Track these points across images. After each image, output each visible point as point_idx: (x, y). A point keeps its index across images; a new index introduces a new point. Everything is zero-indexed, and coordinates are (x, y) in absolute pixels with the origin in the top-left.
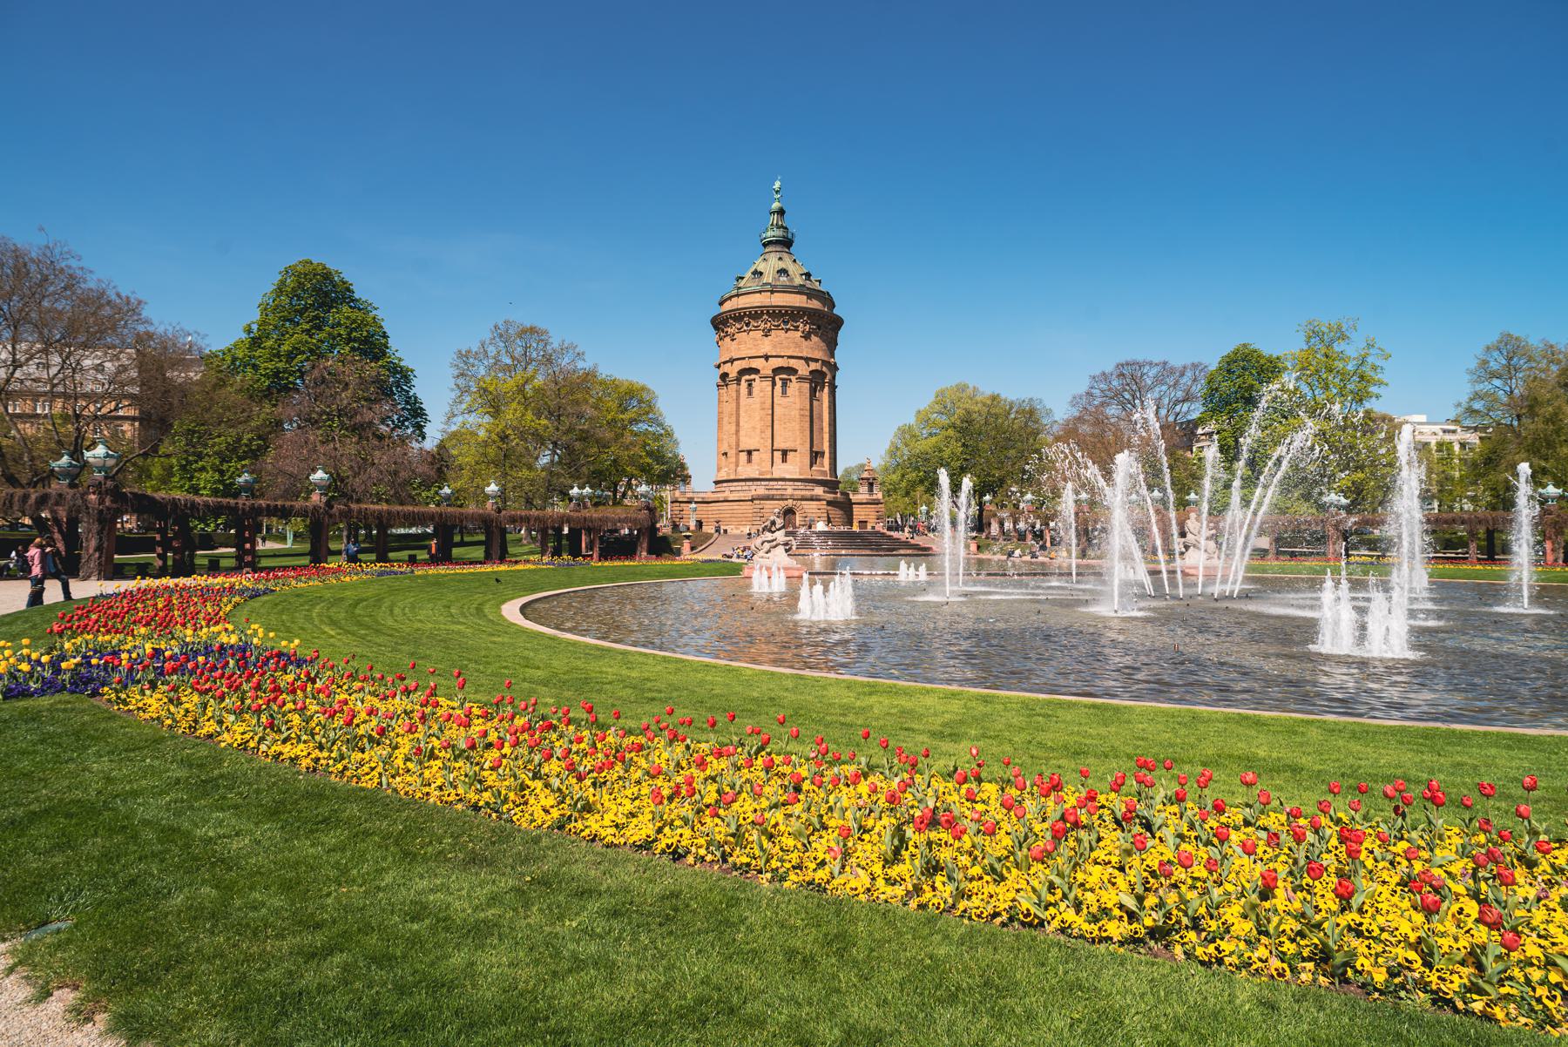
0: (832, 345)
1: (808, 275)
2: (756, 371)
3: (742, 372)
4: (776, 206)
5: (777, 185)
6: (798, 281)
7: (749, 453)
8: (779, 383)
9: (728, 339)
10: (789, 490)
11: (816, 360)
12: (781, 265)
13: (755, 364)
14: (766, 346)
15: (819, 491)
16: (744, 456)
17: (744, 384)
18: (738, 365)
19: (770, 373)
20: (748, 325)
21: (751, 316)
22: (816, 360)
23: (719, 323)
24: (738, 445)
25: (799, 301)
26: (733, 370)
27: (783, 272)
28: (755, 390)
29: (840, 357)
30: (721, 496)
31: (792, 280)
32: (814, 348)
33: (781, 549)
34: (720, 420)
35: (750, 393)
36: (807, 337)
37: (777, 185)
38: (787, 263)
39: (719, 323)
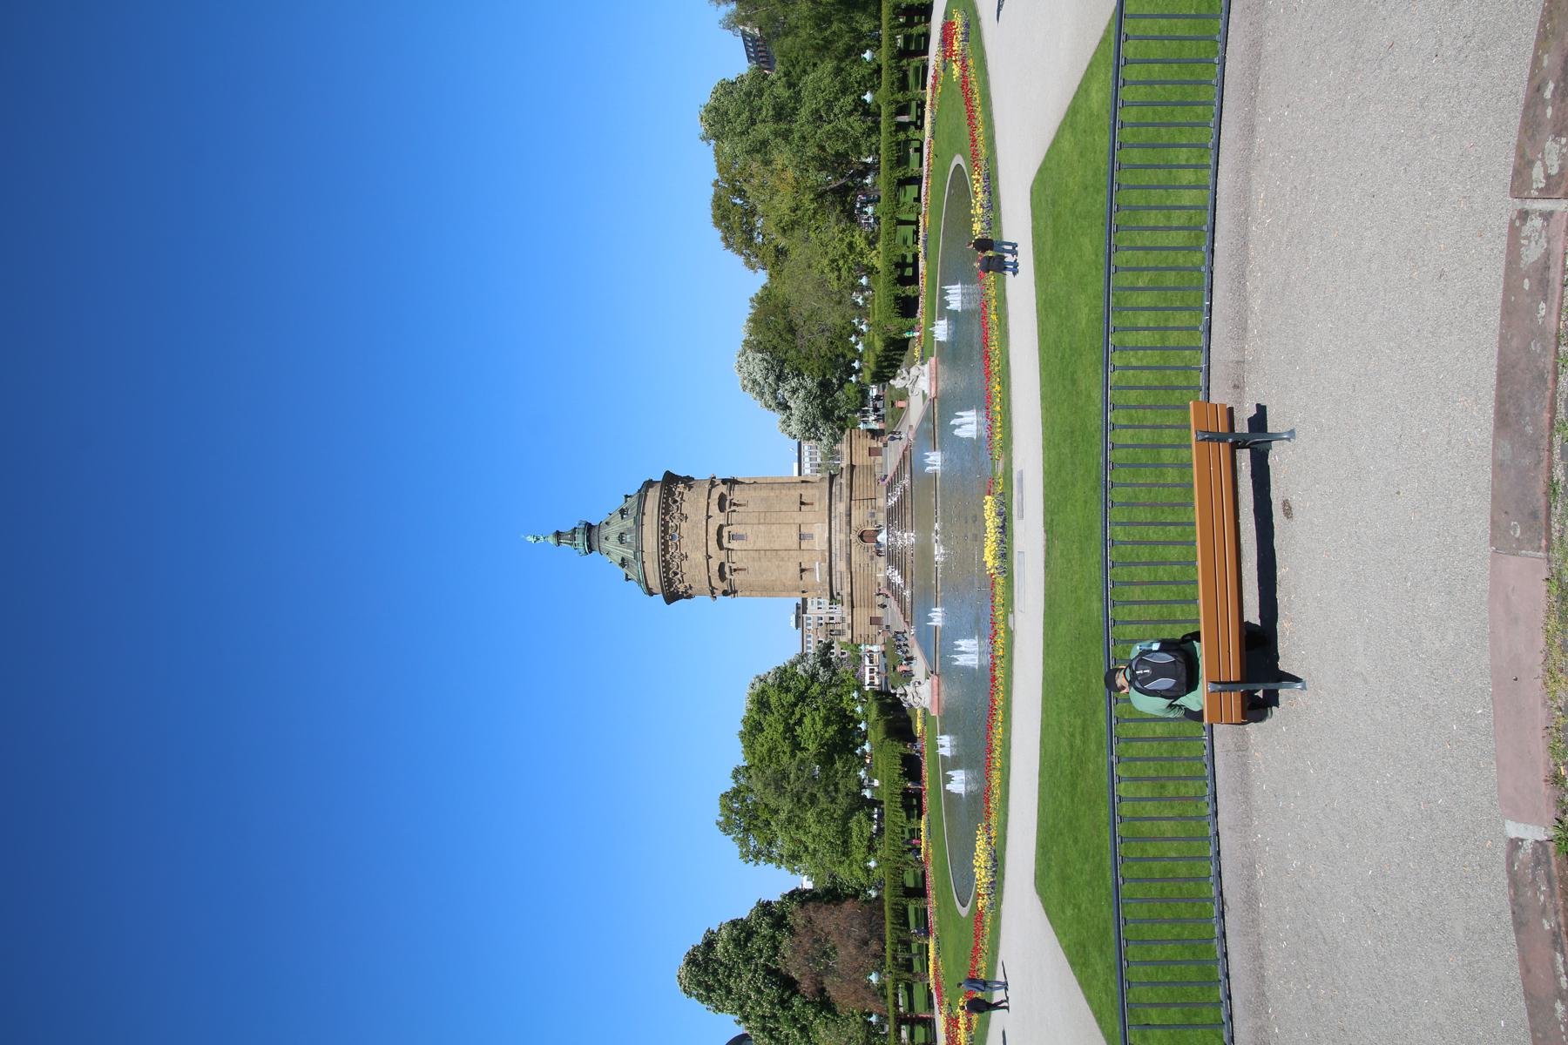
0: (688, 481)
1: (622, 512)
2: (722, 566)
3: (722, 577)
4: (552, 540)
5: (531, 539)
6: (630, 523)
7: (802, 570)
8: (734, 545)
10: (839, 537)
12: (614, 538)
13: (715, 567)
14: (698, 557)
15: (840, 508)
16: (805, 575)
18: (716, 582)
19: (723, 552)
23: (671, 597)
27: (621, 539)
29: (701, 473)
30: (846, 599)
31: (630, 530)
33: (920, 689)
38: (612, 532)
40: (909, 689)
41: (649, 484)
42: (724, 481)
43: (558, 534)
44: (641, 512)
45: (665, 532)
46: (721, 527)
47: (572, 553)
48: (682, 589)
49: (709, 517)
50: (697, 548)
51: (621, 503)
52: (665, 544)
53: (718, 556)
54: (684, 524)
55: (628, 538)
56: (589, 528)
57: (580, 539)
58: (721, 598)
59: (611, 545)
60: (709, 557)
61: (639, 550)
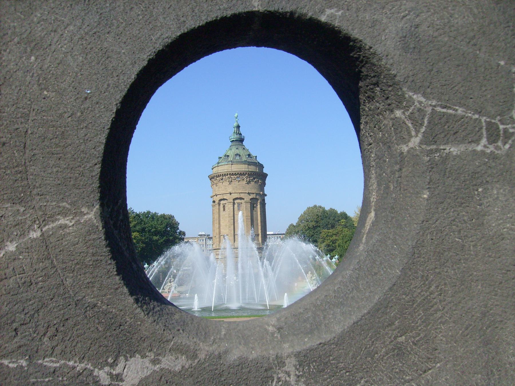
0: (264, 184)
1: (249, 155)
4: (235, 124)
5: (236, 115)
6: (244, 159)
9: (215, 186)
11: (254, 193)
12: (238, 152)
14: (230, 190)
17: (222, 206)
19: (232, 201)
20: (222, 179)
22: (254, 193)
23: (211, 178)
24: (220, 233)
25: (243, 168)
26: (217, 199)
28: (226, 208)
29: (267, 190)
31: (241, 159)
32: (252, 188)
34: (213, 222)
35: (224, 210)
36: (249, 183)
38: (240, 151)
39: (211, 178)
41: (261, 166)
42: (264, 200)
43: (238, 127)
44: (250, 164)
46: (244, 199)
48: (215, 182)
50: (234, 189)
51: (253, 154)
52: (235, 174)
53: (230, 198)
54: (245, 182)
55: (238, 158)
56: (241, 140)
58: (212, 200)
59: (234, 151)
60: (231, 194)
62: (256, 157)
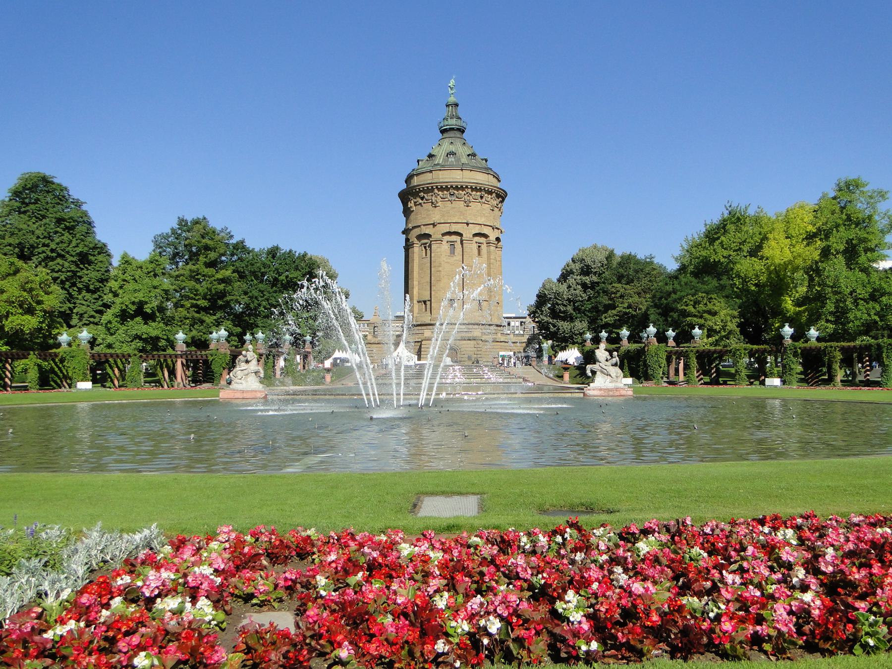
1: (474, 155)
5: (452, 83)
6: (464, 160)
8: (445, 247)
12: (452, 148)
14: (436, 217)
20: (422, 198)
21: (424, 191)
23: (405, 196)
37: (452, 83)
38: (458, 147)
40: (253, 366)
42: (498, 239)
45: (457, 188)
46: (460, 235)
47: (439, 115)
49: (468, 224)
50: (443, 216)
52: (447, 189)
55: (452, 159)
57: (453, 122)
59: (446, 146)
61: (443, 168)
62: (486, 161)
